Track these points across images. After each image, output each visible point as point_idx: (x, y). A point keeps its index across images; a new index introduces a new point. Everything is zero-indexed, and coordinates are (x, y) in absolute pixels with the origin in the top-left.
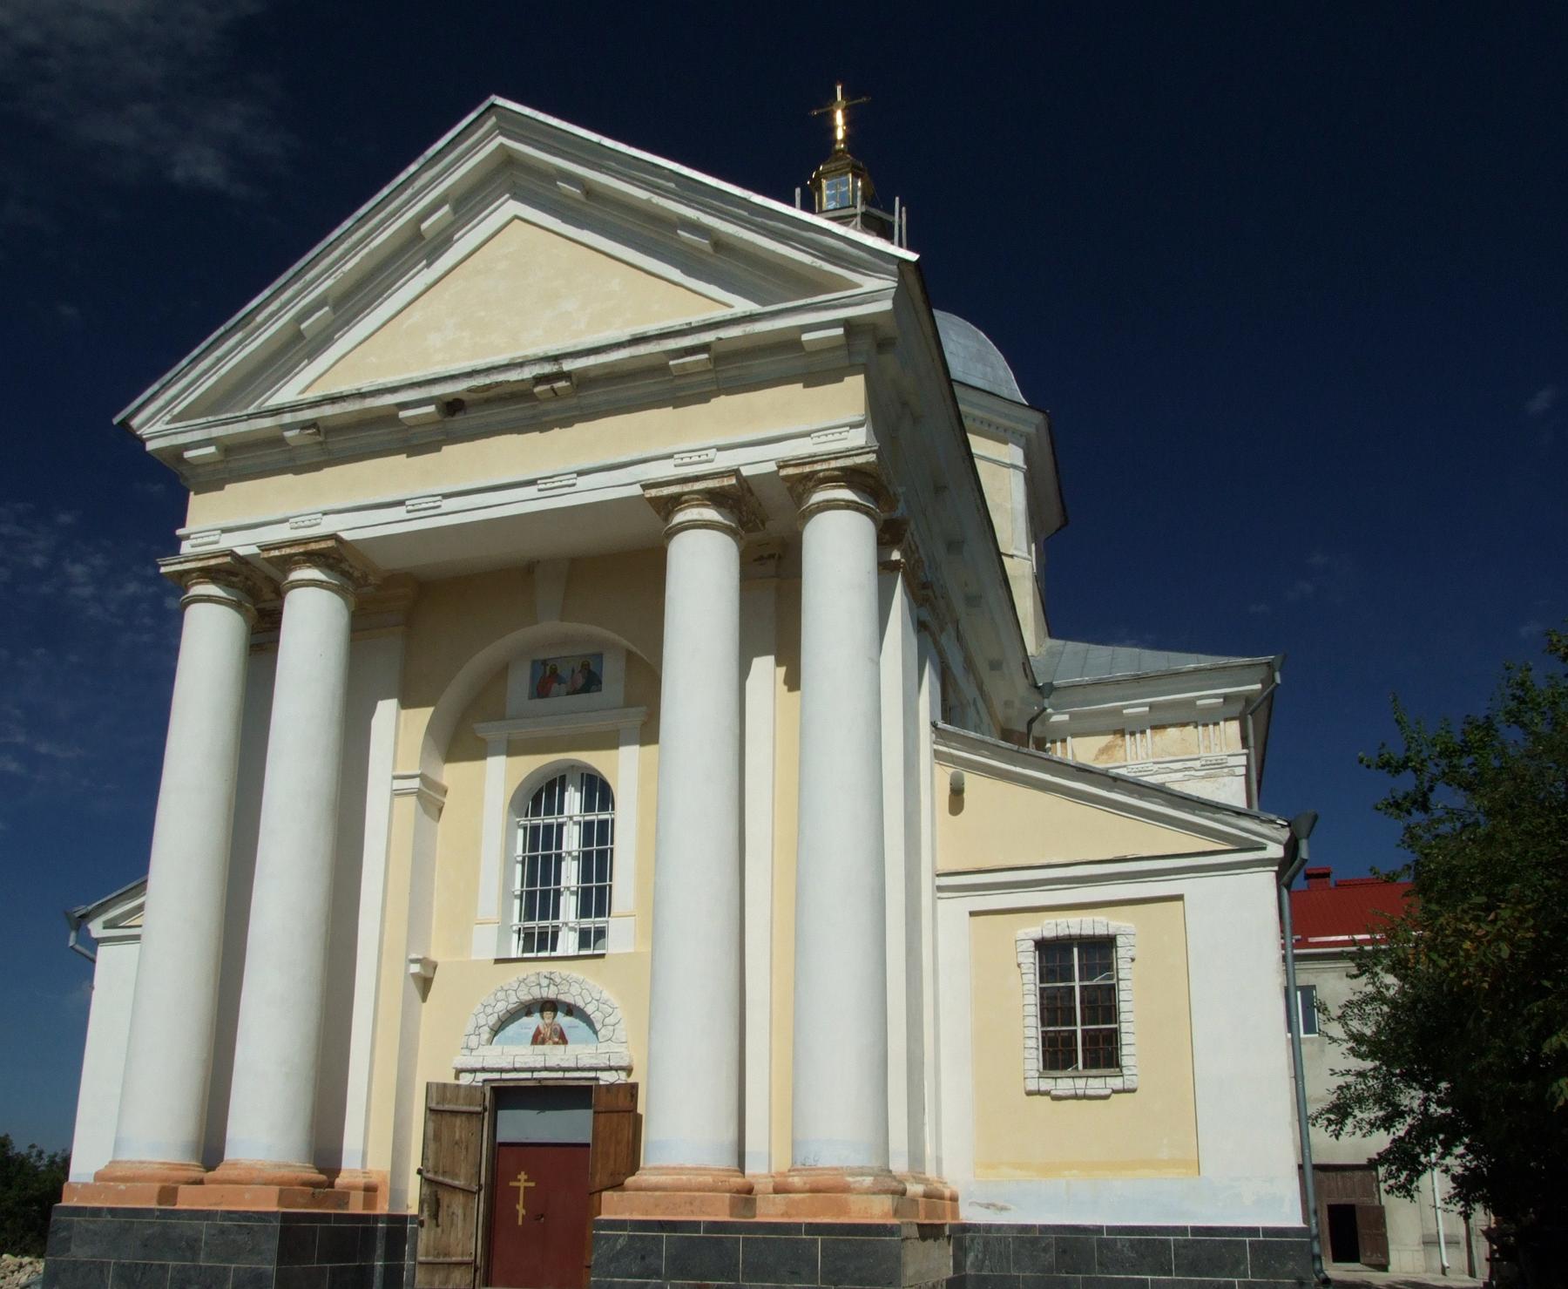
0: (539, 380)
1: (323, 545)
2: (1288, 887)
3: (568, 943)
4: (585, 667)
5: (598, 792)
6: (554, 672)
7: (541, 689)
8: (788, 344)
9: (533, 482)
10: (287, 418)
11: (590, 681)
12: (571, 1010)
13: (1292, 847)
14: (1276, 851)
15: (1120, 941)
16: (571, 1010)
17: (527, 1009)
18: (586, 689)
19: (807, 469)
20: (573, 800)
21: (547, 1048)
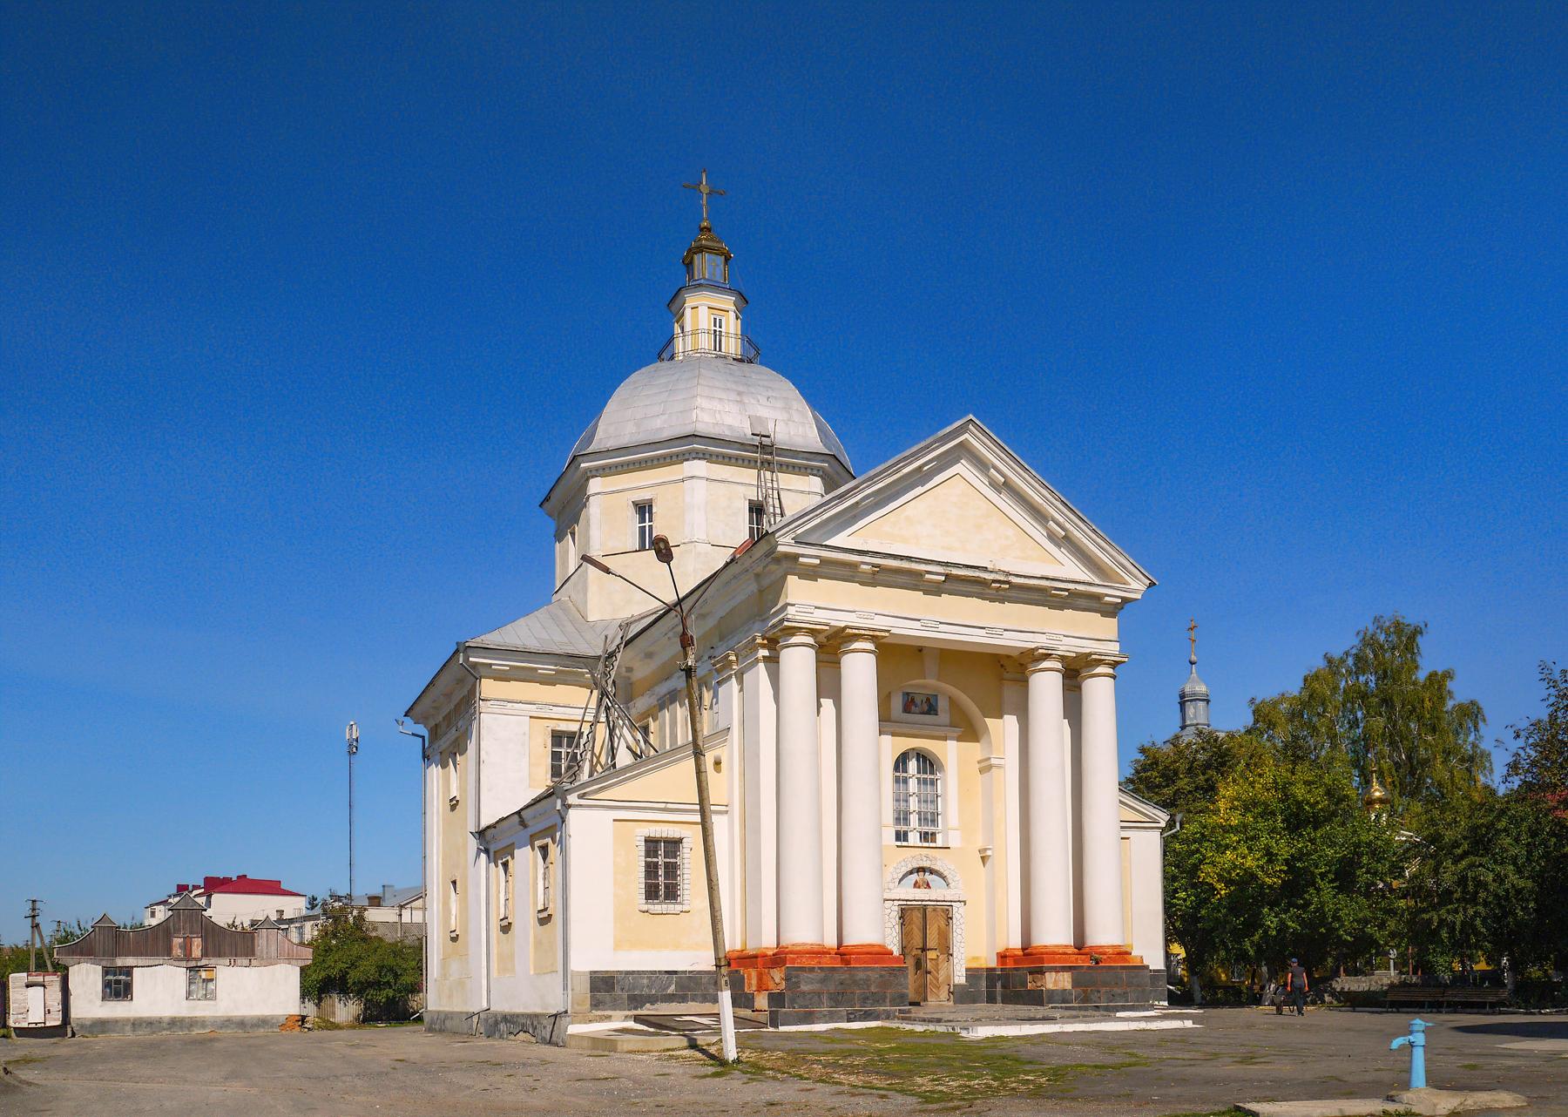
3: (914, 838)
5: (928, 763)
8: (1097, 598)
10: (867, 559)
11: (931, 709)
12: (932, 872)
13: (1171, 824)
14: (1163, 824)
16: (932, 872)
17: (911, 872)
18: (928, 713)
20: (912, 765)
21: (922, 890)
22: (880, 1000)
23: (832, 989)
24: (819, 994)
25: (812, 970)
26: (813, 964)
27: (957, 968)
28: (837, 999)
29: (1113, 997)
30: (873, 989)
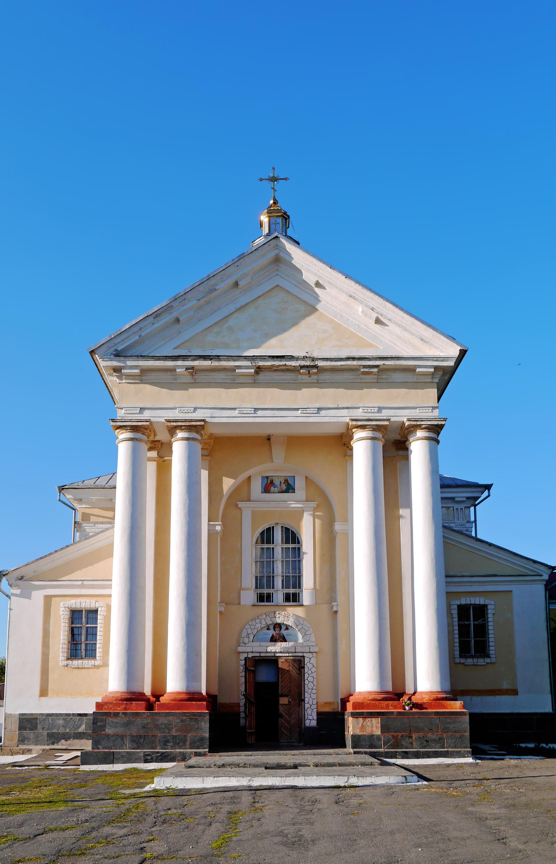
0: (302, 367)
1: (198, 423)
2: (549, 590)
4: (286, 481)
6: (272, 483)
7: (266, 489)
9: (297, 409)
10: (180, 363)
11: (289, 488)
15: (489, 607)
18: (286, 491)
19: (419, 423)
22: (180, 742)
23: (134, 731)
24: (122, 737)
25: (116, 715)
26: (119, 710)
27: (309, 711)
28: (137, 741)
29: (426, 743)
30: (174, 733)
